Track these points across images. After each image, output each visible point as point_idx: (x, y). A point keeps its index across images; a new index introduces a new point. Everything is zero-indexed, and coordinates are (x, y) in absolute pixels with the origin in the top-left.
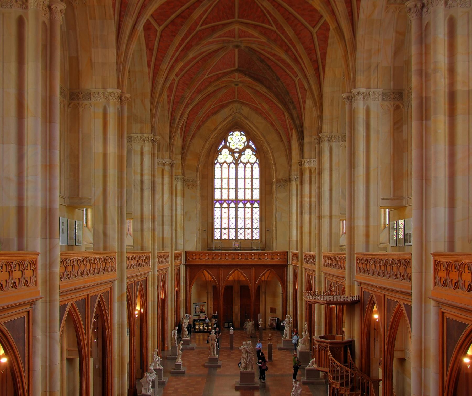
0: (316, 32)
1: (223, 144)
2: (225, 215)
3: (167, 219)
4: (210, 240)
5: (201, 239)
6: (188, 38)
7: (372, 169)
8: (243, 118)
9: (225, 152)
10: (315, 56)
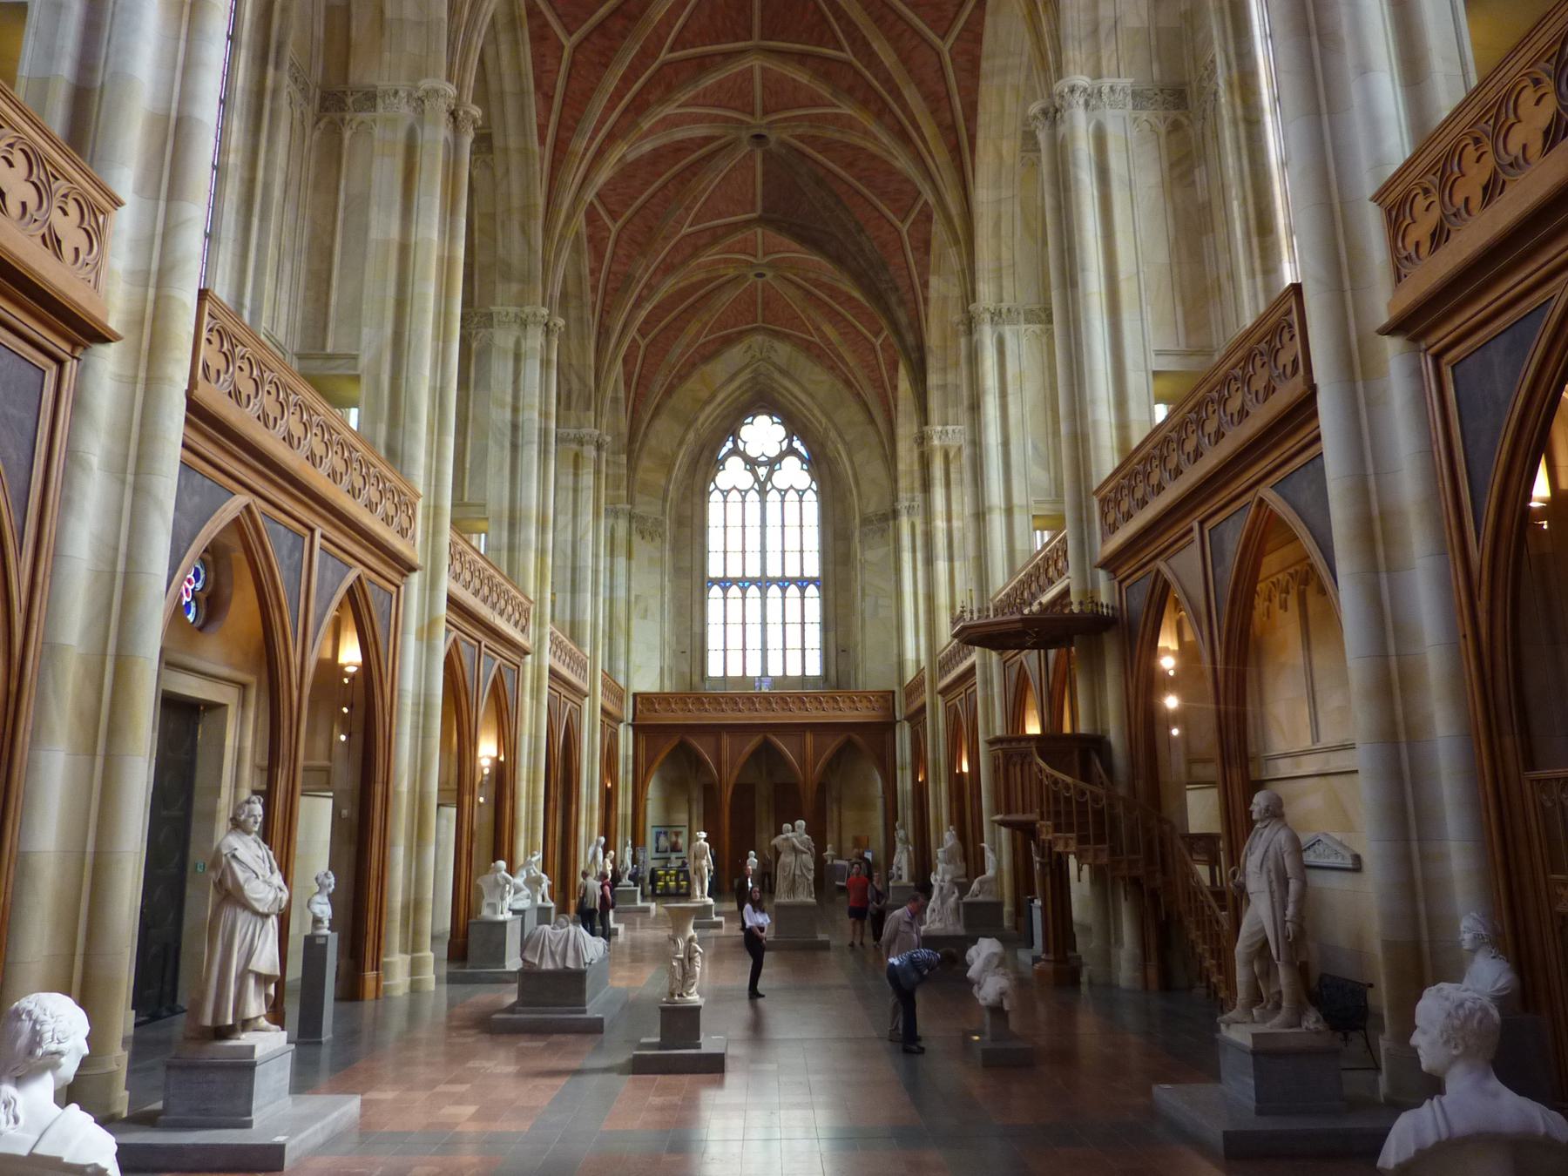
1: (729, 445)
4: (696, 678)
5: (674, 669)
8: (777, 375)
9: (734, 464)
10: (948, 115)
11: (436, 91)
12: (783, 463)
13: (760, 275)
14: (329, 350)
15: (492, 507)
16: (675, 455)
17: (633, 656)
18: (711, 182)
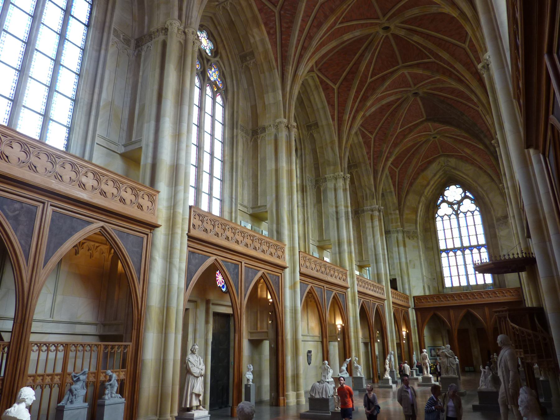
0: (468, 46)
1: (441, 199)
4: (441, 288)
6: (362, 90)
8: (453, 170)
11: (281, 122)
12: (463, 202)
13: (435, 137)
14: (259, 205)
15: (332, 240)
16: (418, 208)
17: (411, 282)
18: (403, 113)
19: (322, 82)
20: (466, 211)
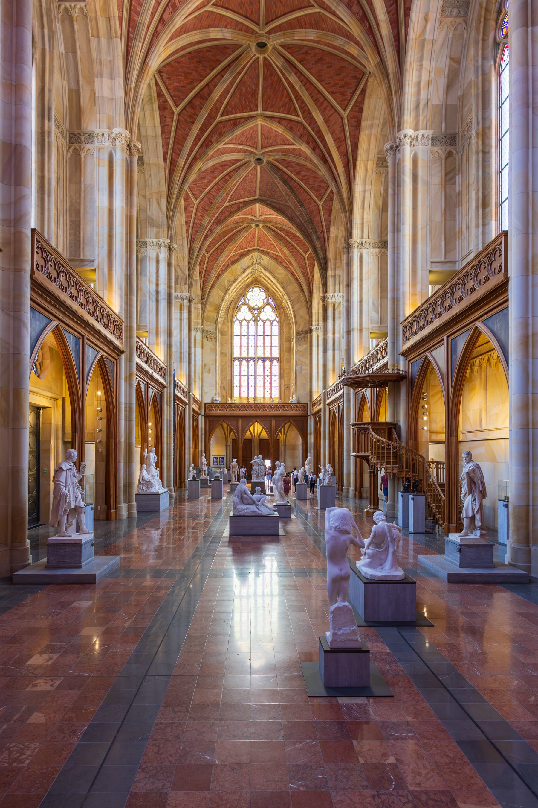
0: (347, 116)
1: (243, 300)
2: (244, 373)
3: (185, 355)
7: (419, 227)
9: (244, 309)
19: (160, 94)
20: (265, 319)
